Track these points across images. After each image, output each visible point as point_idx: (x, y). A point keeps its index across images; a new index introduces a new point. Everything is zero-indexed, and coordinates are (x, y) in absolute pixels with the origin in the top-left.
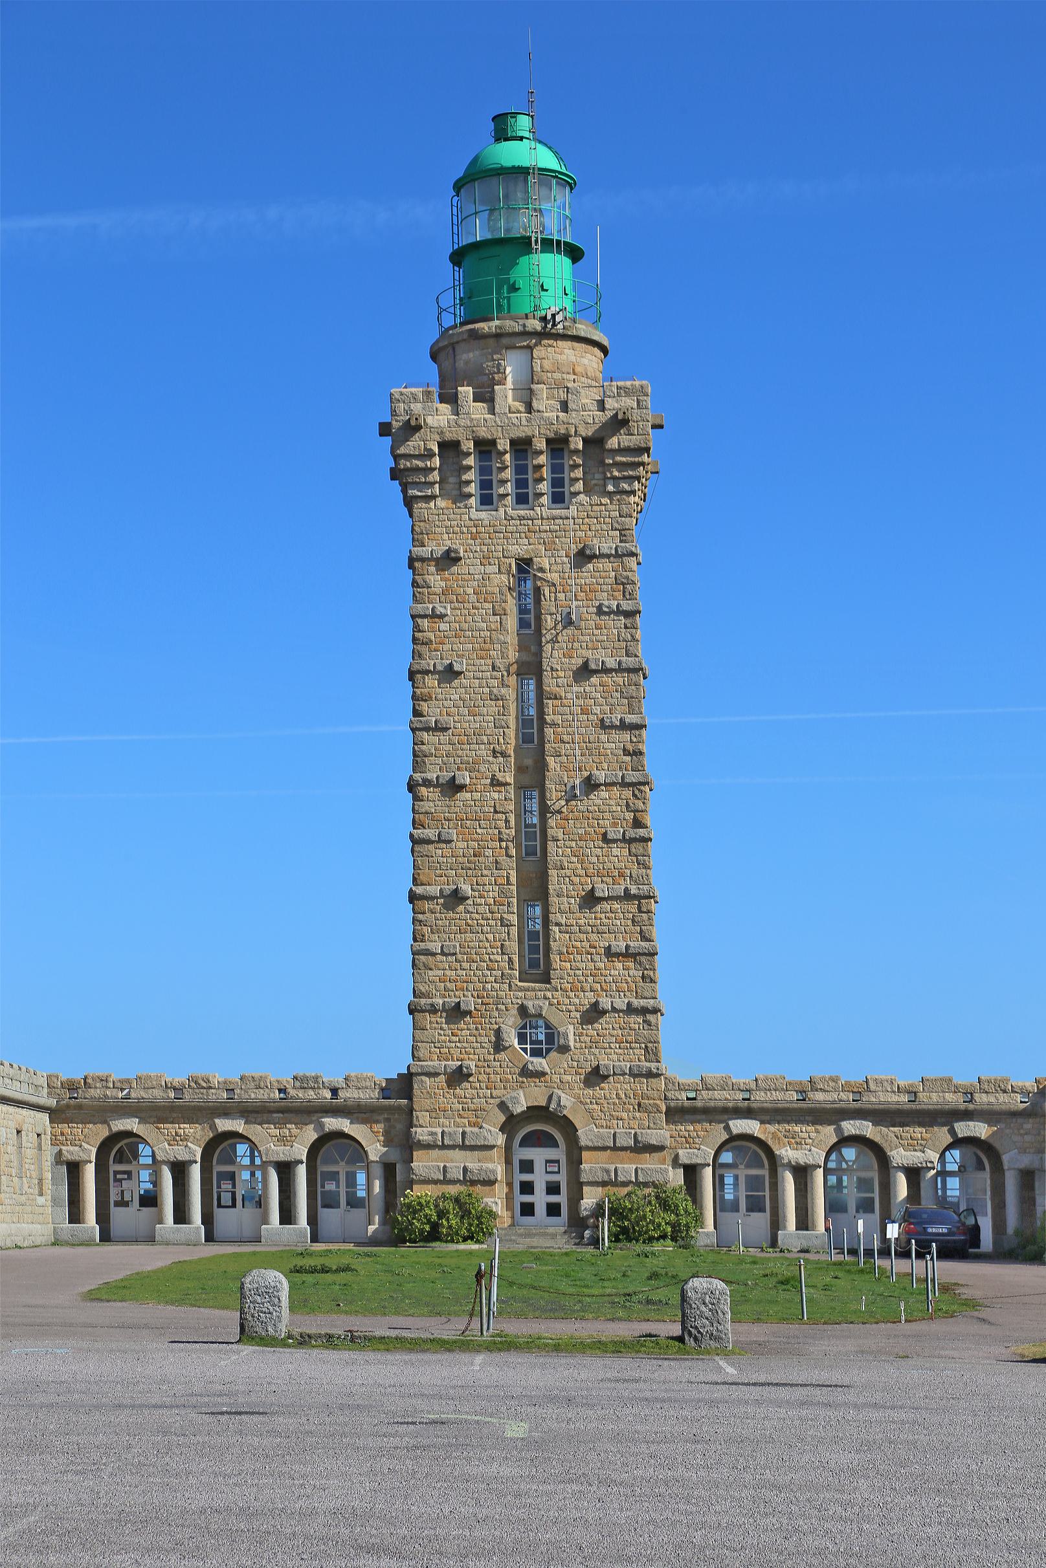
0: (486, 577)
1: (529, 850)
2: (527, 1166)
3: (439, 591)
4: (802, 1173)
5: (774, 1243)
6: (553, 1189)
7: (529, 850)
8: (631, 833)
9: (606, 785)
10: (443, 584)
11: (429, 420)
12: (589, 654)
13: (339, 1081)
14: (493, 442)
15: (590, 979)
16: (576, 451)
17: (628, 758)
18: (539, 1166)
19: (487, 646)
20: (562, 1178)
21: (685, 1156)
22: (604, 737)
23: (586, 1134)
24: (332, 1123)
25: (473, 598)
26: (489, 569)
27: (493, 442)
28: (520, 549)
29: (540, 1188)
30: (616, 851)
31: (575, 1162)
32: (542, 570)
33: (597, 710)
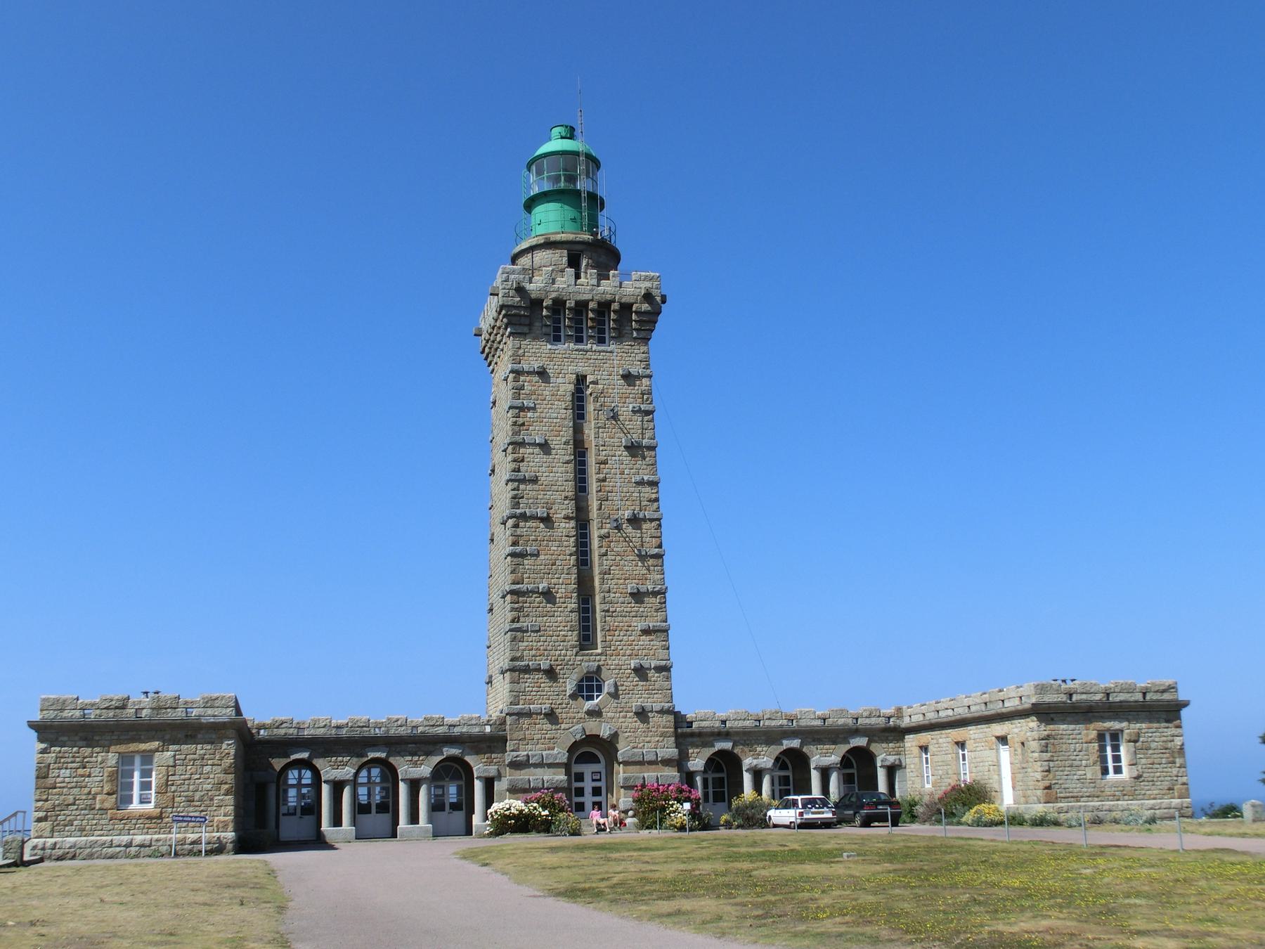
1: (582, 563)
2: (580, 777)
7: (582, 563)
18: (588, 777)
20: (602, 784)
22: (632, 489)
29: (588, 791)
31: (610, 772)
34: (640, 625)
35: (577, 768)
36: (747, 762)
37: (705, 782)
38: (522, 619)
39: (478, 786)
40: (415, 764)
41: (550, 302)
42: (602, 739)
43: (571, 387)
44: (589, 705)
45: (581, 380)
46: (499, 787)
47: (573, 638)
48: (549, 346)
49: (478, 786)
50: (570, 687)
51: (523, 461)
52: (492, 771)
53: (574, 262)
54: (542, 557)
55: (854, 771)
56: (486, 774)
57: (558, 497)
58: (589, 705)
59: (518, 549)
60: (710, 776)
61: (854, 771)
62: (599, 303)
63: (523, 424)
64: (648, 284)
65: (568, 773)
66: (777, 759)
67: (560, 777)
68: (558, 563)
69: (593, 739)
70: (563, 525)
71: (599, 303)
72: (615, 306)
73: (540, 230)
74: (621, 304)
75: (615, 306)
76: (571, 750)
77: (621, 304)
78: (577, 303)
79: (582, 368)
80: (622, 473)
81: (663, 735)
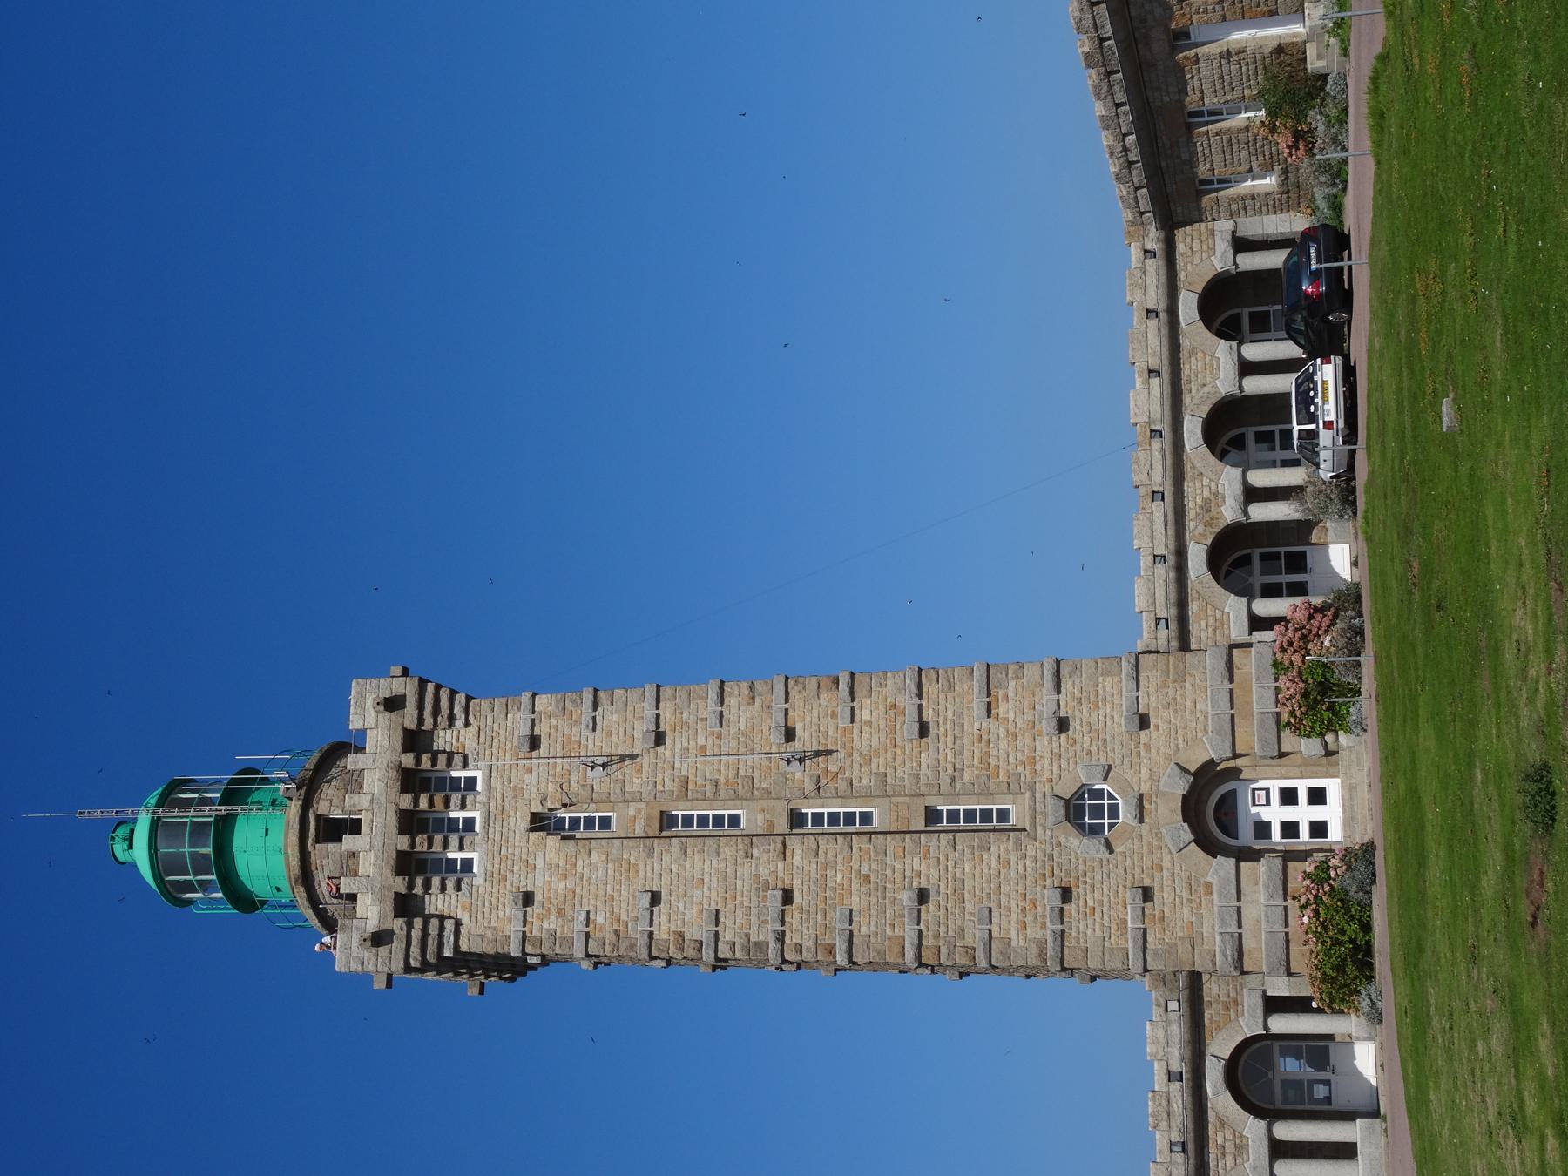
0: (549, 866)
3: (560, 922)
4: (1252, 494)
6: (1289, 797)
10: (552, 918)
13: (1159, 1071)
14: (400, 854)
17: (757, 700)
22: (733, 730)
23: (1208, 749)
25: (570, 883)
26: (540, 863)
27: (401, 855)
29: (1289, 813)
34: (976, 721)
35: (1246, 836)
36: (1230, 512)
37: (1271, 591)
38: (969, 941)
39: (1282, 1024)
40: (1241, 1149)
41: (400, 880)
42: (1193, 787)
43: (553, 842)
44: (1126, 815)
45: (541, 823)
46: (1280, 987)
47: (1001, 847)
48: (478, 881)
49: (1282, 1024)
50: (1090, 848)
51: (681, 935)
52: (1252, 1002)
53: (334, 830)
54: (855, 902)
55: (1245, 313)
56: (1260, 1012)
57: (746, 871)
58: (1126, 815)
60: (1259, 579)
61: (1245, 313)
62: (404, 790)
63: (616, 932)
64: (370, 703)
65: (1253, 856)
66: (1222, 456)
67: (1261, 873)
68: (865, 870)
69: (1191, 808)
70: (797, 859)
71: (404, 790)
72: (408, 760)
73: (285, 885)
74: (405, 750)
75: (408, 760)
76: (1210, 847)
77: (405, 750)
78: (401, 832)
79: (523, 822)
80: (703, 750)
81: (1180, 679)
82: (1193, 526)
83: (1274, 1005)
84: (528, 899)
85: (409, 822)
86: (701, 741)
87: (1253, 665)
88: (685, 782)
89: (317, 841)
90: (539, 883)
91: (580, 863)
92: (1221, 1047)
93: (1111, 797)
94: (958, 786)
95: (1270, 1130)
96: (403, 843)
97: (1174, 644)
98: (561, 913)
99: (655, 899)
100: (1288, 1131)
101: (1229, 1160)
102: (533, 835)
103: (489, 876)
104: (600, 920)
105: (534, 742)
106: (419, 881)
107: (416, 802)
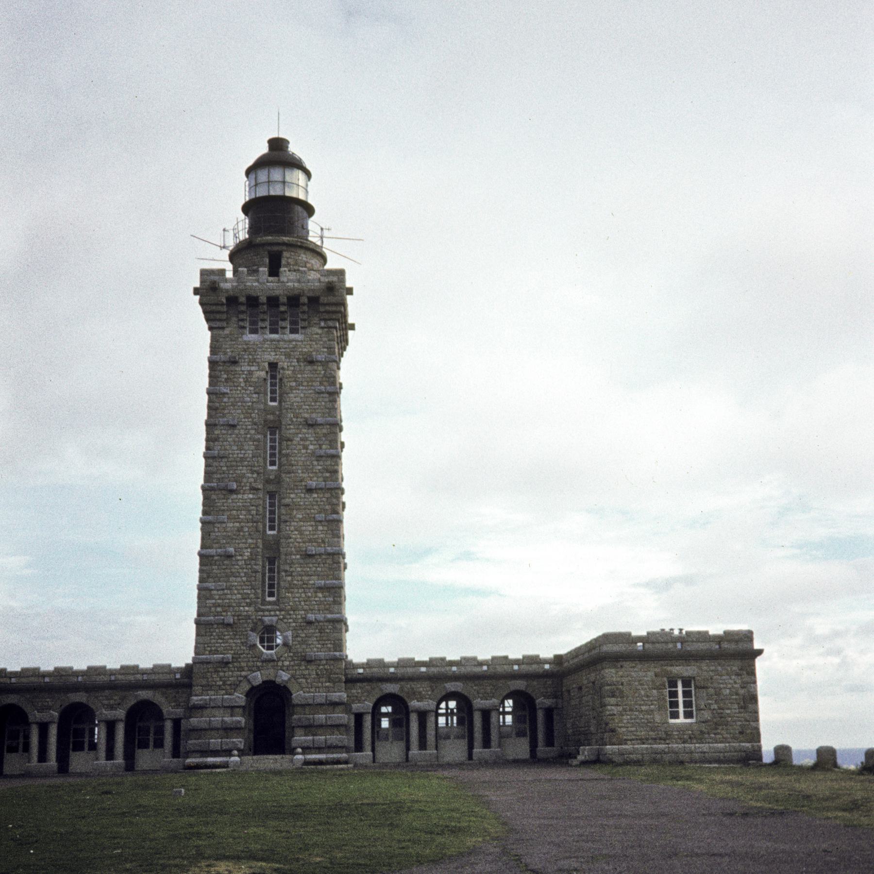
0: (250, 373)
5: (407, 760)
8: (330, 517)
9: (316, 489)
11: (222, 285)
12: (306, 415)
15: (303, 603)
16: (304, 304)
19: (250, 411)
21: (356, 707)
24: (144, 694)
26: (253, 368)
27: (256, 299)
28: (271, 357)
30: (320, 528)
32: (283, 368)
33: (311, 447)
36: (414, 704)
40: (112, 707)
59: (210, 518)
72: (304, 300)
77: (309, 298)
82: (408, 686)
83: (177, 723)
84: (234, 362)
85: (273, 301)
86: (311, 447)
87: (342, 717)
88: (289, 440)
89: (269, 252)
90: (243, 369)
91: (252, 388)
92: (157, 697)
93: (263, 647)
94: (283, 574)
95: (121, 720)
96: (263, 299)
97: (349, 676)
98: (227, 380)
99: (233, 426)
100: (53, 731)
101: (106, 702)
102: (266, 365)
103: (247, 343)
104: (225, 400)
105: (311, 362)
106: (243, 308)
107: (284, 304)
